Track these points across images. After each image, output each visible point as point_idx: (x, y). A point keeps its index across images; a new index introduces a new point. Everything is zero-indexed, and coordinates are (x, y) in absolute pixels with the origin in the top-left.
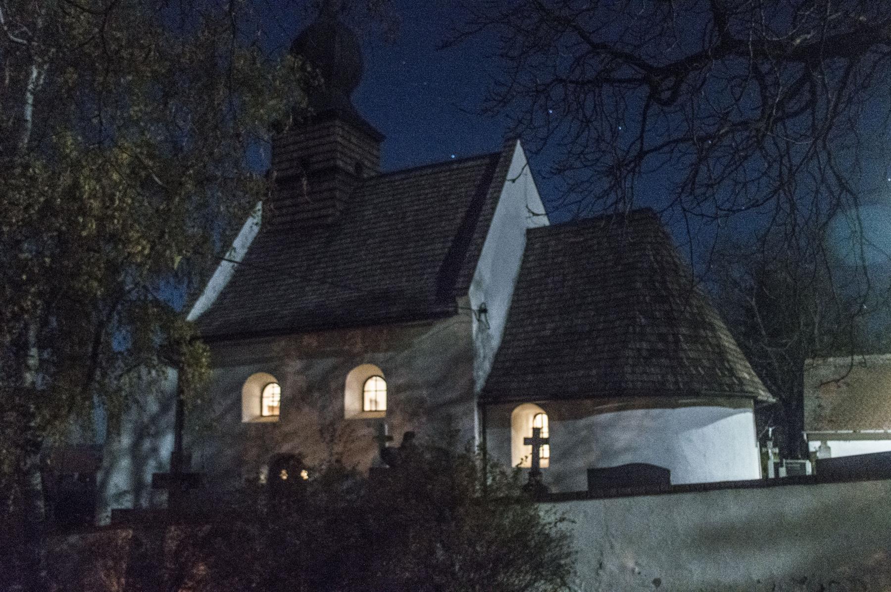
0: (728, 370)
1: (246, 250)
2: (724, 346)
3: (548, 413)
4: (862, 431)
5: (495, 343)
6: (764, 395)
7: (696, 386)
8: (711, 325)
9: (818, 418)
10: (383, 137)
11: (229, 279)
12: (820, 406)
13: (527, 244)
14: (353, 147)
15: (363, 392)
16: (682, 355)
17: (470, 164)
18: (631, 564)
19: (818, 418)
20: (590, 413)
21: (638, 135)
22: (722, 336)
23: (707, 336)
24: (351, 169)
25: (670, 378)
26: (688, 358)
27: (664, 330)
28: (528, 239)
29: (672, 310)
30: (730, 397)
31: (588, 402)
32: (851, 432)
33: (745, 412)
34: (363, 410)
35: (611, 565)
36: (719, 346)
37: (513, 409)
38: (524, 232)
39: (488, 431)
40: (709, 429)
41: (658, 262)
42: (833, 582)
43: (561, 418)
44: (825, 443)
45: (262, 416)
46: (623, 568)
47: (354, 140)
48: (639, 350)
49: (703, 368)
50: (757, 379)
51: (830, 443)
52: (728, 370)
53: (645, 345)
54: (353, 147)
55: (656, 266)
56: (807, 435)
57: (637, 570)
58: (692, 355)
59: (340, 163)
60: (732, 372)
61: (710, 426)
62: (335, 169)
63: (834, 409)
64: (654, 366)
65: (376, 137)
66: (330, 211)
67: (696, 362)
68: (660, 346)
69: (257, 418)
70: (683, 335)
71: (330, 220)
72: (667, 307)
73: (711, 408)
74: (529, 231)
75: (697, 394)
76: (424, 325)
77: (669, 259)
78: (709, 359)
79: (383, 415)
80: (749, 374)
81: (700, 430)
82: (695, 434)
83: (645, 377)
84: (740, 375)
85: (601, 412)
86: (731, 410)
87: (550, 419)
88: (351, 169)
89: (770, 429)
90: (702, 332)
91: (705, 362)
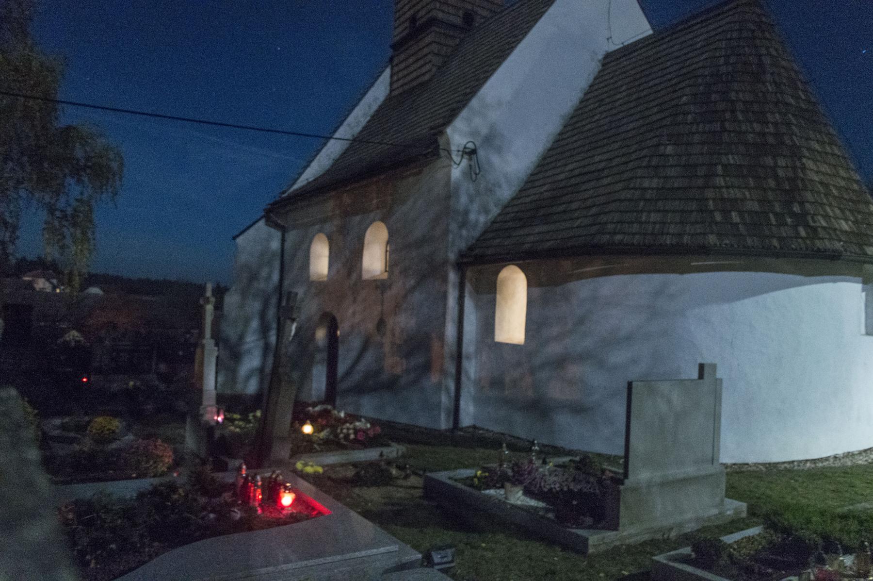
0: (793, 215)
5: (506, 193)
7: (712, 239)
23: (774, 168)
24: (458, 21)
28: (603, 65)
29: (724, 130)
31: (567, 264)
33: (835, 281)
37: (498, 272)
38: (600, 57)
40: (747, 307)
43: (540, 285)
49: (741, 213)
52: (793, 215)
53: (655, 183)
59: (440, 15)
60: (801, 219)
61: (746, 301)
62: (433, 21)
70: (725, 166)
71: (427, 77)
73: (753, 274)
74: (608, 55)
75: (704, 251)
76: (415, 174)
81: (726, 306)
86: (799, 278)
87: (529, 285)
88: (458, 21)
90: (769, 161)
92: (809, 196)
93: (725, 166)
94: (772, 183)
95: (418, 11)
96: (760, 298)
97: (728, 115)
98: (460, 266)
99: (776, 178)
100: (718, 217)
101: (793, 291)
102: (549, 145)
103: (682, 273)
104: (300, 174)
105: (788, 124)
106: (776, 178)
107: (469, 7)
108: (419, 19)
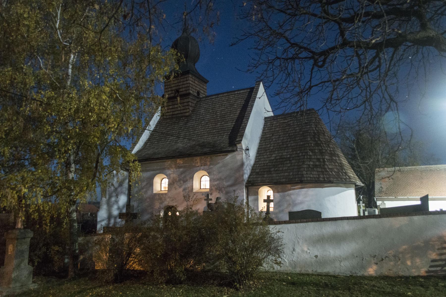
1: (155, 126)
2: (343, 163)
3: (273, 190)
4: (398, 197)
5: (252, 162)
6: (359, 183)
7: (332, 179)
8: (338, 154)
9: (381, 192)
10: (208, 81)
11: (148, 137)
12: (381, 187)
13: (265, 123)
14: (196, 85)
15: (201, 181)
16: (326, 167)
17: (241, 92)
18: (306, 249)
19: (381, 192)
20: (290, 190)
21: (309, 79)
22: (342, 159)
23: (336, 160)
25: (322, 176)
26: (329, 168)
27: (318, 157)
28: (265, 121)
29: (322, 149)
30: (345, 183)
31: (289, 186)
32: (394, 197)
34: (200, 189)
35: (298, 250)
36: (341, 163)
38: (264, 118)
39: (249, 197)
40: (337, 196)
41: (316, 130)
42: (387, 257)
43: (278, 192)
44: (383, 202)
45: (161, 191)
46: (303, 251)
47: (196, 82)
48: (309, 165)
49: (335, 172)
50: (356, 177)
51: (385, 202)
53: (311, 163)
54: (196, 85)
55: (316, 131)
56: (376, 199)
57: (308, 251)
58: (330, 167)
59: (191, 92)
60: (346, 173)
61: (337, 195)
62: (189, 94)
63: (387, 188)
64: (315, 171)
65: (205, 81)
66: (188, 110)
67: (332, 170)
68: (317, 163)
69: (159, 191)
70: (327, 159)
71: (187, 114)
72: (320, 148)
74: (266, 118)
76: (223, 155)
77: (321, 129)
78: (337, 169)
79: (208, 190)
80: (353, 174)
81: (333, 197)
82: (331, 198)
83: (312, 176)
84: (350, 175)
85: (294, 189)
87: (274, 192)
88: (196, 94)
89: (361, 196)
91: (335, 170)
92: (345, 168)
93: (327, 159)
94: (337, 164)
95: (179, 89)
96: (339, 194)
97: (322, 144)
98: (247, 187)
99: (338, 163)
100: (331, 174)
101: (345, 192)
102: (258, 147)
103: (322, 188)
104: (133, 148)
105: (334, 148)
106: (338, 163)
107: (198, 89)
108: (181, 92)
